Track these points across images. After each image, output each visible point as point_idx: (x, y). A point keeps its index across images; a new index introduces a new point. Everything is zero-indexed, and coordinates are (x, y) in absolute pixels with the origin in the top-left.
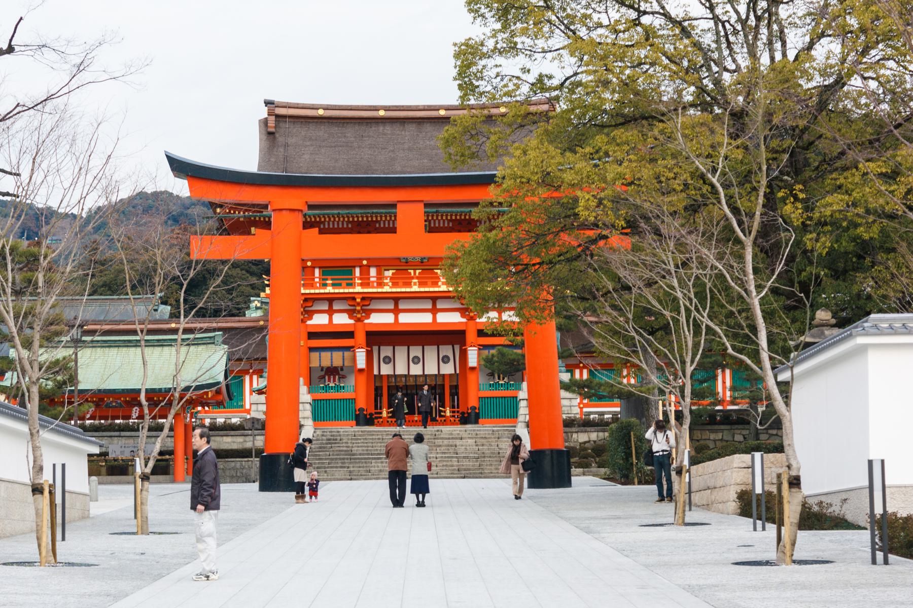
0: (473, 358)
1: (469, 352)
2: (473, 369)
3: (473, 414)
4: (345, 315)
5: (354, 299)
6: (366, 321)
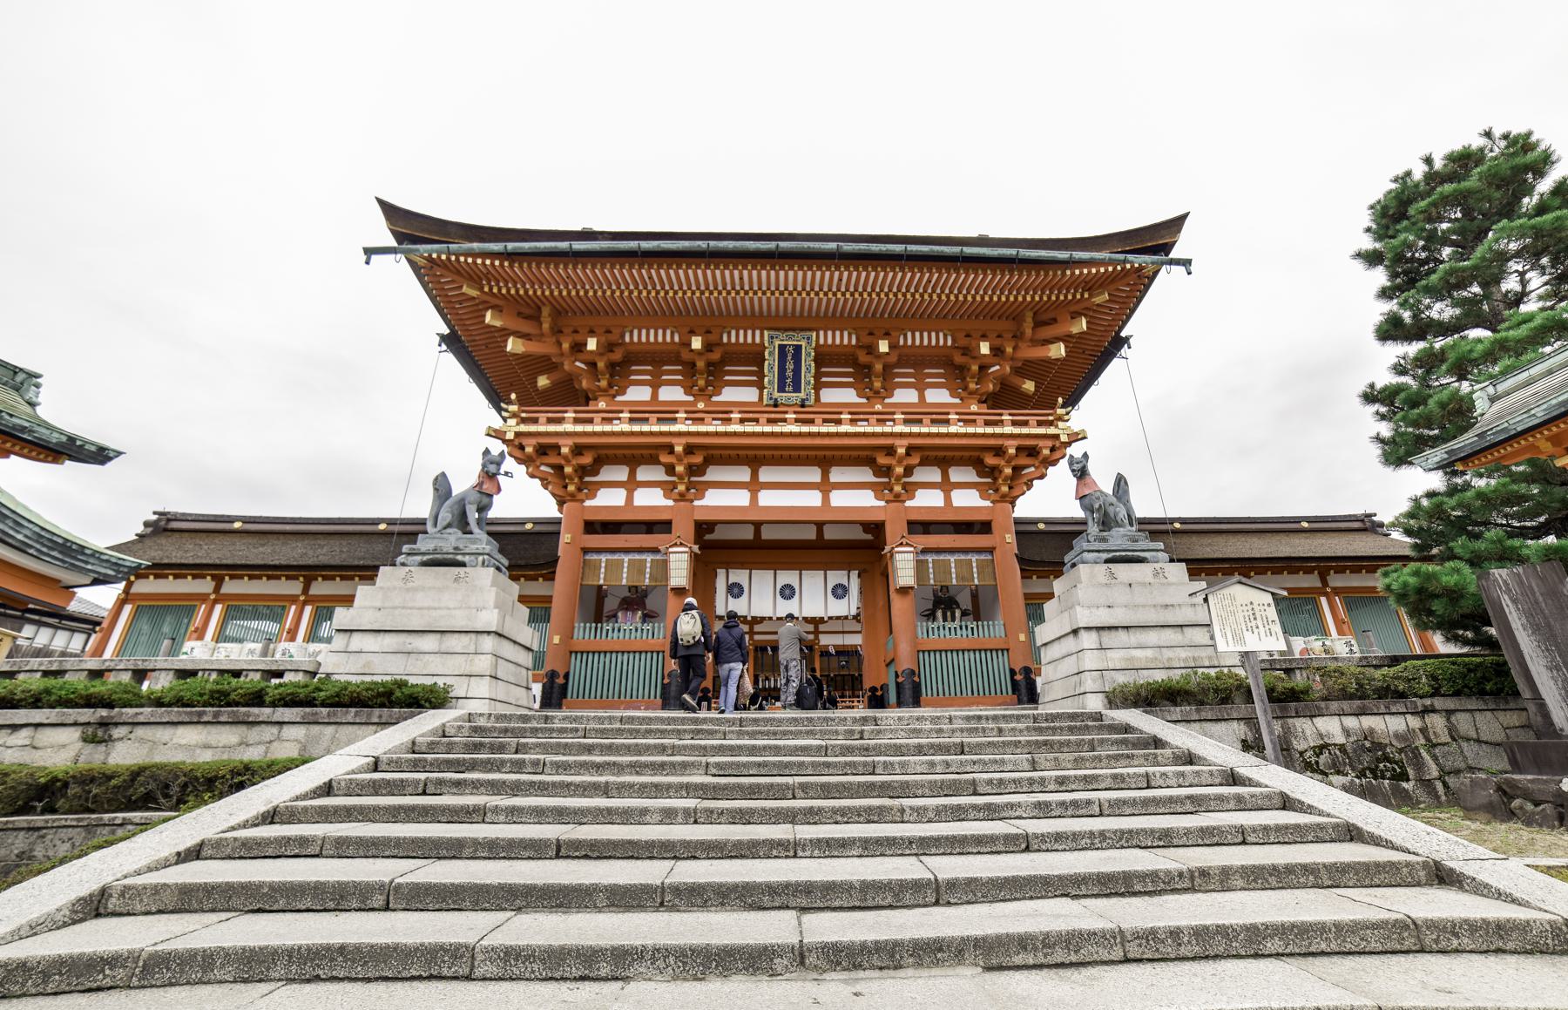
0: (904, 568)
1: (898, 557)
2: (904, 591)
3: (908, 686)
4: (659, 492)
5: (670, 449)
6: (696, 503)
